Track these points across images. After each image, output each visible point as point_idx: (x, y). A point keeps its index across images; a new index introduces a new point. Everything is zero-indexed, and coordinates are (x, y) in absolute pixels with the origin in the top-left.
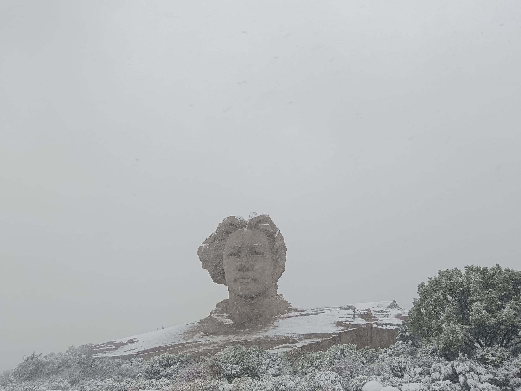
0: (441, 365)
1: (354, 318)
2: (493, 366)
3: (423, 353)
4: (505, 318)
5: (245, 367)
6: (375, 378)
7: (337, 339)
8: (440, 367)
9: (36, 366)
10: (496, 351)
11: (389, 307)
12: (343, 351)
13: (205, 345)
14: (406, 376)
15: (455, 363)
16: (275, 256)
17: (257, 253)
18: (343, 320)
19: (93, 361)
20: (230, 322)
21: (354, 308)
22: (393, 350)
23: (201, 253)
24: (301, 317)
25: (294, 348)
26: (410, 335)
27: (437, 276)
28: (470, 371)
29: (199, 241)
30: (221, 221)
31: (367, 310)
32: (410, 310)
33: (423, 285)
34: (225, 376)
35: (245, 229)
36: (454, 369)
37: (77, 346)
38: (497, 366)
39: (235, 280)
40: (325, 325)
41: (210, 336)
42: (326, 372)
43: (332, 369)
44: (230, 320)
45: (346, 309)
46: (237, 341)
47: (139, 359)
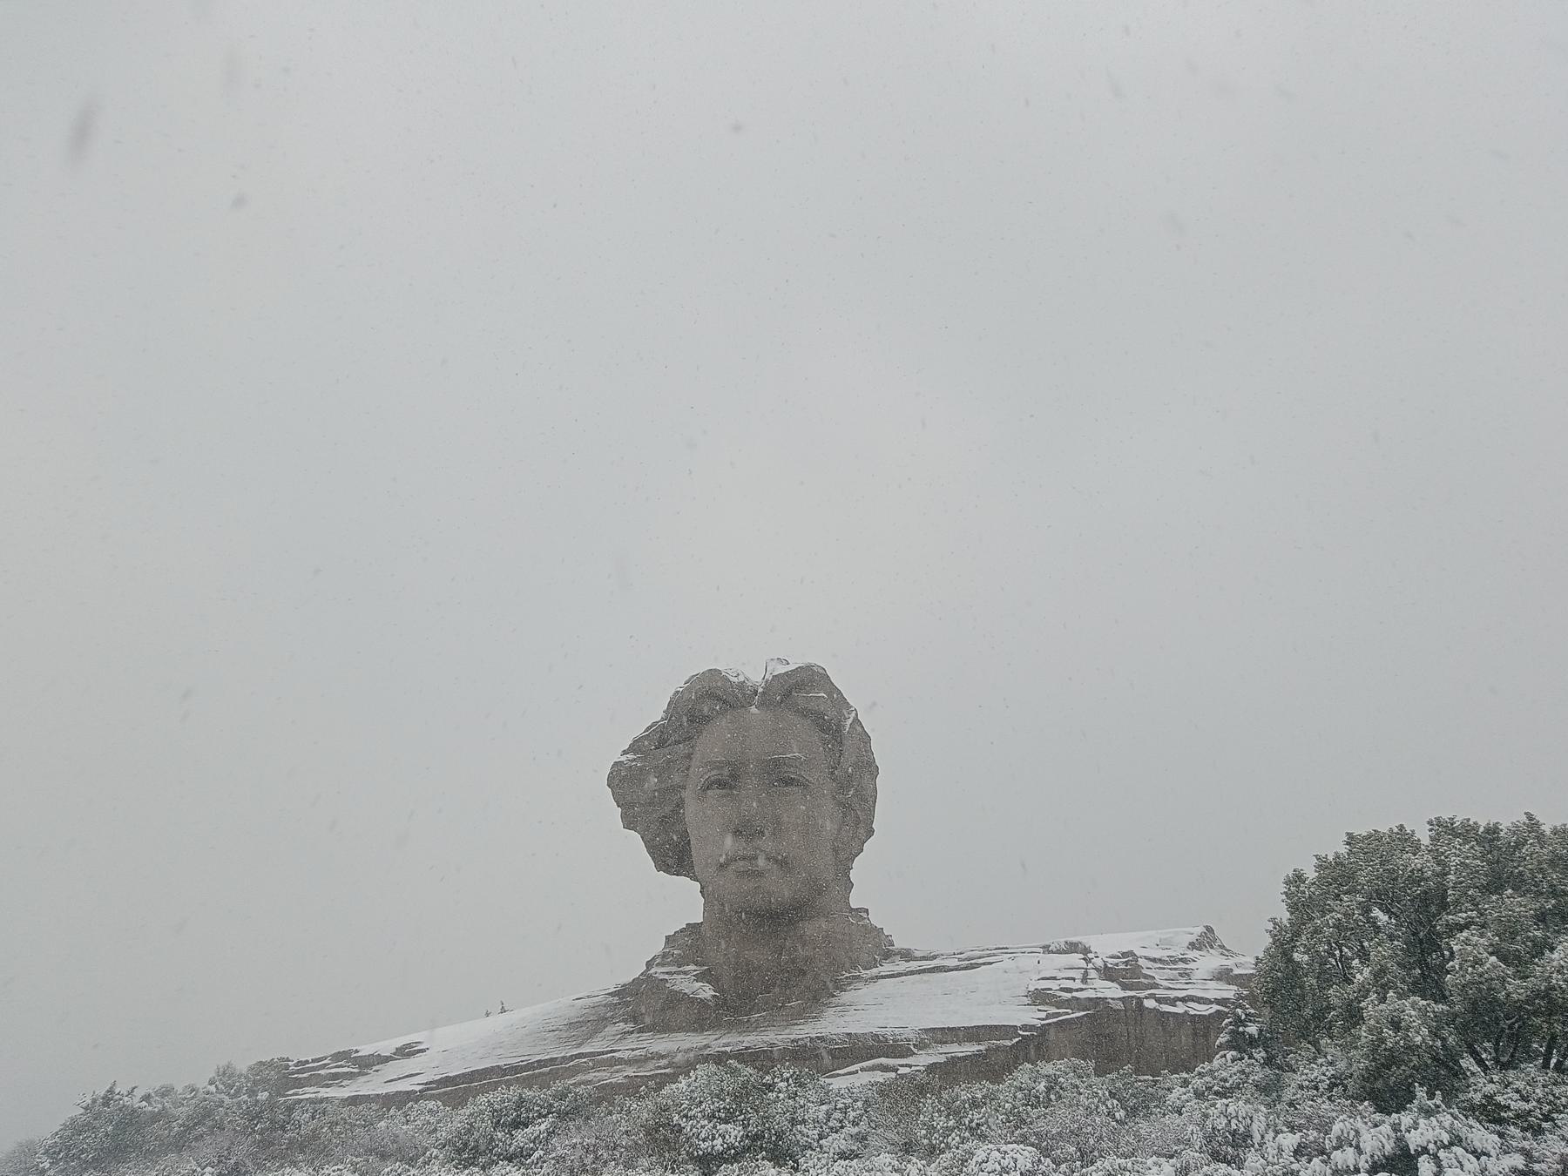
0: (1359, 1124)
1: (1085, 979)
2: (1524, 1130)
3: (1301, 1087)
4: (1557, 979)
5: (753, 1129)
6: (1155, 1164)
7: (1032, 1045)
8: (1357, 1132)
9: (116, 1127)
10: (1532, 1083)
11: (1192, 946)
12: (1053, 1084)
13: (629, 1062)
14: (1252, 1159)
15: (1406, 1119)
16: (843, 788)
17: (789, 782)
18: (1054, 985)
19: (290, 1109)
20: (706, 992)
21: (1086, 951)
22: (1208, 1079)
23: (622, 781)
25: (902, 1071)
26: (1261, 1030)
27: (1343, 850)
28: (1451, 1144)
29: (614, 746)
30: (679, 683)
31: (1124, 955)
32: (1261, 956)
33: (1298, 878)
34: (692, 1158)
35: (753, 709)
36: (1399, 1140)
37: (242, 1066)
38: (1538, 1131)
40: (997, 1000)
42: (1004, 1148)
43: (1022, 1135)
44: (707, 987)
45: (1059, 952)
47: (431, 1104)
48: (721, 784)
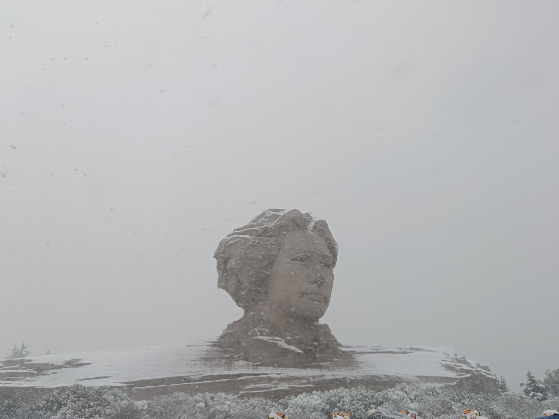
39: (303, 295)
41: (270, 368)
46: (338, 377)
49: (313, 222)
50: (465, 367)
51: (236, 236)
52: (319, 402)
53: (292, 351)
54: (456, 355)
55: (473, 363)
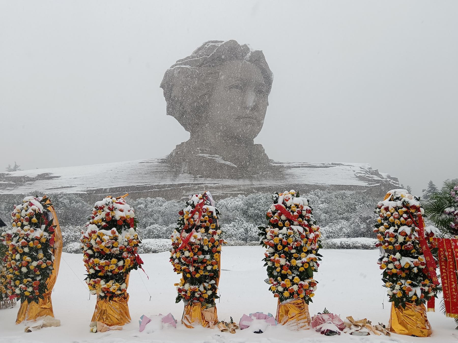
24: (311, 169)
39: (239, 118)
41: (208, 179)
48: (237, 87)
49: (250, 53)
50: (376, 178)
51: (178, 66)
52: (240, 203)
53: (228, 166)
54: (370, 168)
55: (384, 175)
